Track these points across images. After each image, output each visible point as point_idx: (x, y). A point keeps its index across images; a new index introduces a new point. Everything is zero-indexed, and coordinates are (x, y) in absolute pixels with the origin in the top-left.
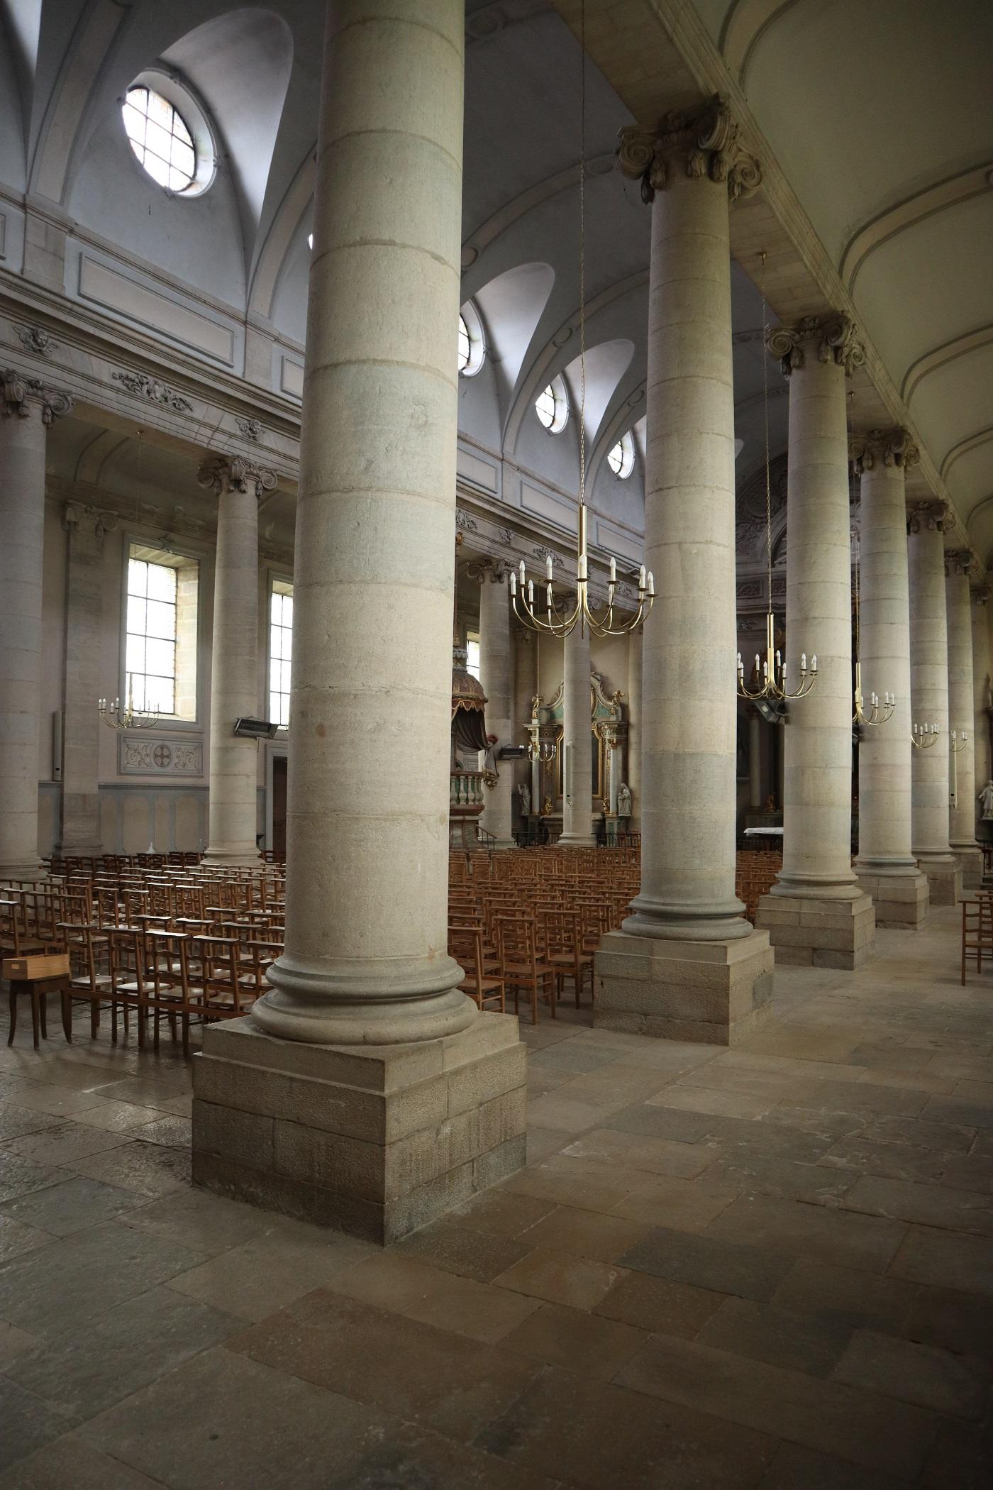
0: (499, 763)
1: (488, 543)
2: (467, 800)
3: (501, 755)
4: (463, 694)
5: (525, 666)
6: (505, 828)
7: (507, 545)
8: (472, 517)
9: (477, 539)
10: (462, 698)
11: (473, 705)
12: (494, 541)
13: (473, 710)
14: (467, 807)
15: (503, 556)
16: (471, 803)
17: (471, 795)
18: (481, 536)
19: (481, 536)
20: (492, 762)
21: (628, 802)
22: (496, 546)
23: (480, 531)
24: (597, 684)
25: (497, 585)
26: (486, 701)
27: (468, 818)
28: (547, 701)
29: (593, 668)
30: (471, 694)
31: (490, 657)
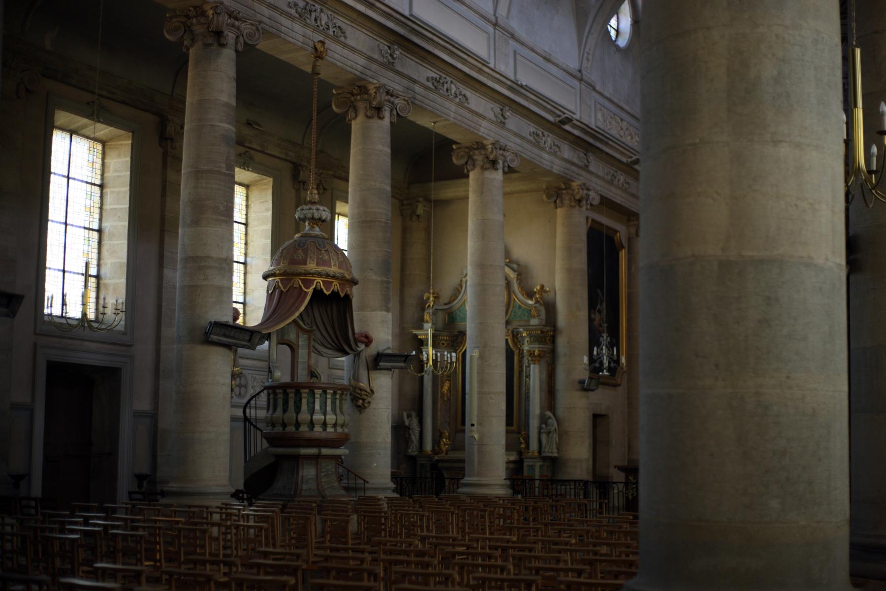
0: (374, 375)
1: (362, 61)
2: (325, 424)
3: (378, 362)
4: (320, 269)
5: (417, 251)
6: (380, 469)
7: (389, 66)
8: (340, 21)
9: (346, 52)
10: (320, 275)
11: (336, 286)
12: (370, 59)
13: (335, 294)
14: (324, 435)
15: (383, 81)
16: (330, 429)
17: (331, 418)
18: (353, 50)
19: (353, 50)
20: (363, 373)
21: (555, 437)
22: (374, 67)
23: (351, 42)
24: (512, 275)
25: (375, 123)
26: (354, 282)
27: (325, 451)
28: (445, 298)
29: (507, 253)
30: (334, 269)
31: (359, 227)
